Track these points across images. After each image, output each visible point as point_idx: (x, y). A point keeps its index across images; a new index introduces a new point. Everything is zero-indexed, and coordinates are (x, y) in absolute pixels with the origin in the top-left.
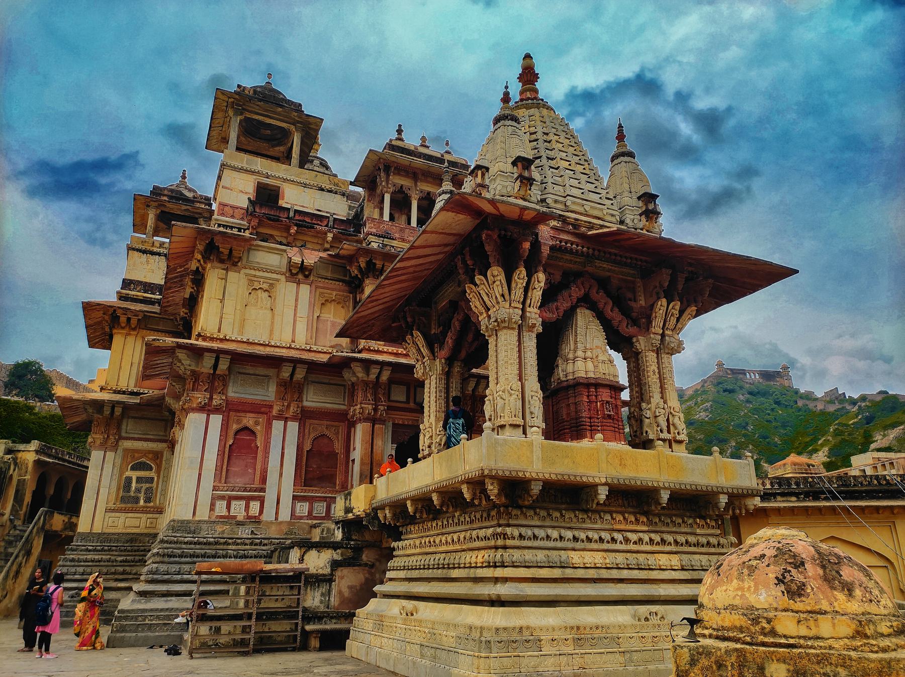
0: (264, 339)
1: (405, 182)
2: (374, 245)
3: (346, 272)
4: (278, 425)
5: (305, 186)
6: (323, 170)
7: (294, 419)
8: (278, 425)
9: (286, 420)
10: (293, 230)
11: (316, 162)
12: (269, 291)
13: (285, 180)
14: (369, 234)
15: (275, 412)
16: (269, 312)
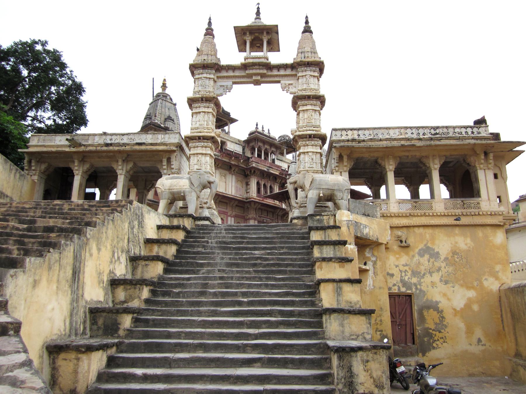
0: (224, 192)
1: (260, 144)
2: (254, 165)
3: (245, 173)
4: (229, 218)
5: (232, 142)
6: (170, 101)
7: (233, 217)
8: (229, 218)
9: (231, 217)
10: (233, 158)
11: (168, 97)
12: (225, 176)
13: (228, 140)
14: (253, 161)
15: (229, 214)
16: (224, 183)
